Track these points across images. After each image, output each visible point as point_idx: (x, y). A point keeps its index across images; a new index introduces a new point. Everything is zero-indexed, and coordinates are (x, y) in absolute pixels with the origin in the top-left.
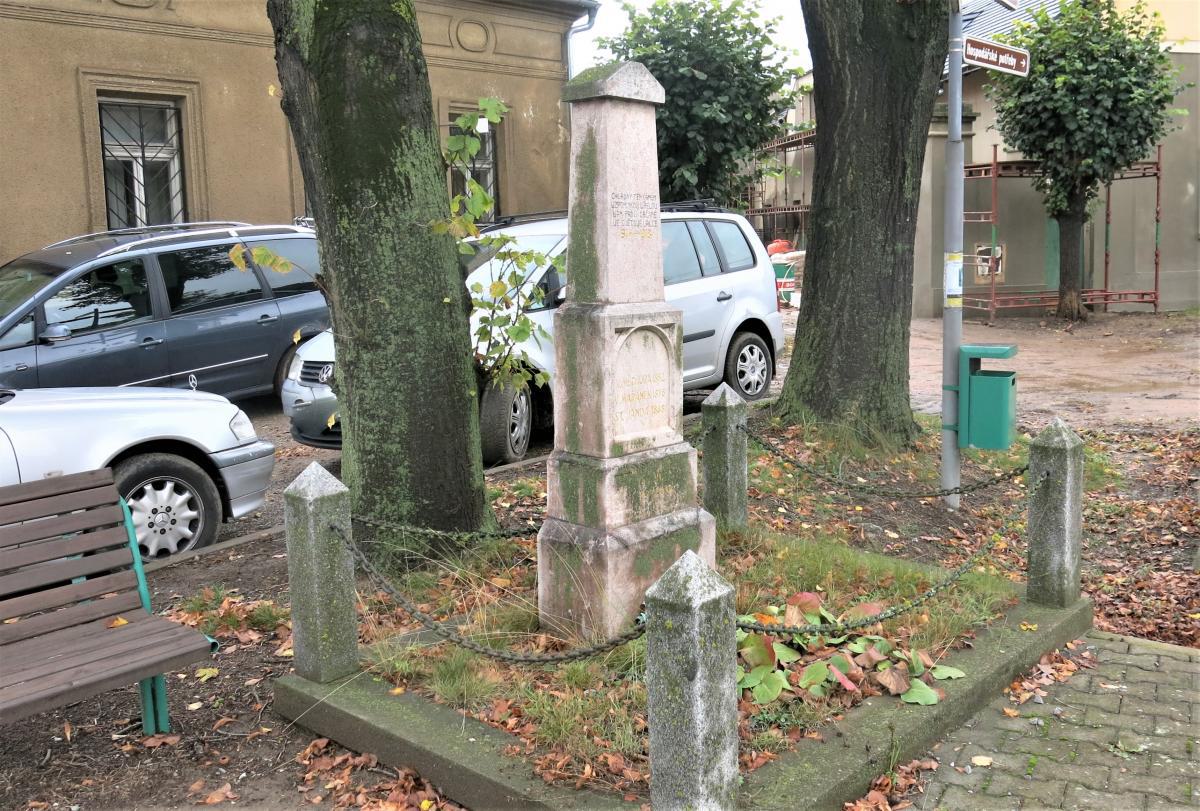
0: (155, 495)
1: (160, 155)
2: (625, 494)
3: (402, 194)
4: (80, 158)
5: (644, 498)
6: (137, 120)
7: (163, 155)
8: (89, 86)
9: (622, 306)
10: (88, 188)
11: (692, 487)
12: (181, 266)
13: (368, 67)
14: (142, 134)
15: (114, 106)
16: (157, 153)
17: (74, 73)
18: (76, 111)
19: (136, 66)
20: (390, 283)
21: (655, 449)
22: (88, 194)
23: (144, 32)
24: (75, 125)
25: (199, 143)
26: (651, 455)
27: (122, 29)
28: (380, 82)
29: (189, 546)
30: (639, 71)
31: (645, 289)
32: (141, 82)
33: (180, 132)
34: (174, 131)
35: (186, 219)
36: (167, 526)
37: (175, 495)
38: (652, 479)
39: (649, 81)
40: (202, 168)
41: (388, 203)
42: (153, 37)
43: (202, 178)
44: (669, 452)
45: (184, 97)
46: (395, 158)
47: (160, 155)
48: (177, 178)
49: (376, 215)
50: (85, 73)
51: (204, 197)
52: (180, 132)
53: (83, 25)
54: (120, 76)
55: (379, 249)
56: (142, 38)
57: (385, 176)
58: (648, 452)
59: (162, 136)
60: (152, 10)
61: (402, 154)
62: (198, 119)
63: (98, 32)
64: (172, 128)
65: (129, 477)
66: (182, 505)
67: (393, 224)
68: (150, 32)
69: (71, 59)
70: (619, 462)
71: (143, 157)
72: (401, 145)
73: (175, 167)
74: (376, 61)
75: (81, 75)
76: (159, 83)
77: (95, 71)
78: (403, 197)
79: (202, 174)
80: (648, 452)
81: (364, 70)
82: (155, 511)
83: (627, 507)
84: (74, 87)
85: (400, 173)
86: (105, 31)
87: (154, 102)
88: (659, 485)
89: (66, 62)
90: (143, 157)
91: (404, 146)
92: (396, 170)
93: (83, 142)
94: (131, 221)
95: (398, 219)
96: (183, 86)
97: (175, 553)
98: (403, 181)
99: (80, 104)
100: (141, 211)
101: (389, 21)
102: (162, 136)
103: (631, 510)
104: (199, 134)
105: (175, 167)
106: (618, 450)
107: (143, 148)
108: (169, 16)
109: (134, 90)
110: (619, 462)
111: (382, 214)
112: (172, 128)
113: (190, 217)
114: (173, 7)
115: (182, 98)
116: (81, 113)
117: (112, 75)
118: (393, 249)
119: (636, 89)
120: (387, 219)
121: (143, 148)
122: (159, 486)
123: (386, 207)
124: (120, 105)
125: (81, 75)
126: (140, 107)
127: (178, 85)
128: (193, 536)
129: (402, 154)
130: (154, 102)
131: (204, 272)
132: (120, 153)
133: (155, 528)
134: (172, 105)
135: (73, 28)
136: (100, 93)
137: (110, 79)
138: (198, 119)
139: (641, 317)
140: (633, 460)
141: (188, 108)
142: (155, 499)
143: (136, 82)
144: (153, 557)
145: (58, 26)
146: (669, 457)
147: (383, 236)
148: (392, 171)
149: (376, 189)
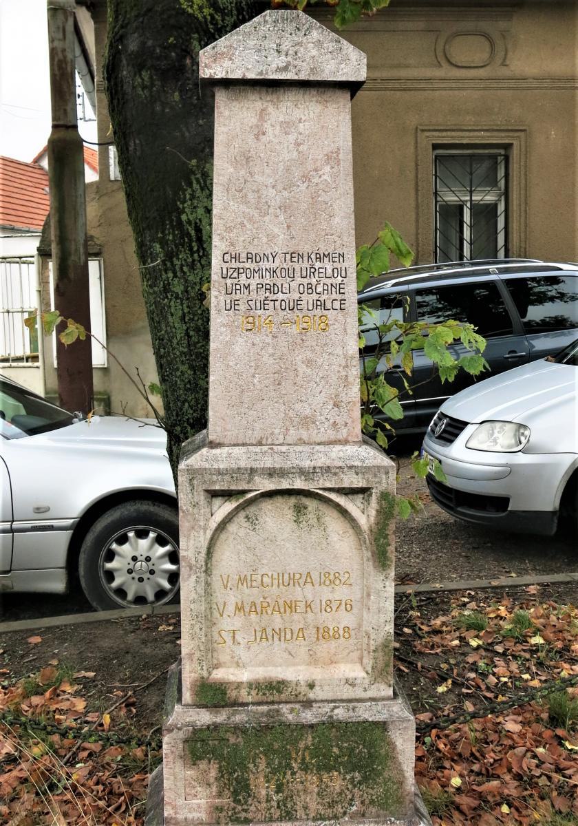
0: (137, 544)
1: (487, 198)
2: (213, 773)
3: (191, 249)
4: (413, 203)
5: (262, 788)
6: (469, 170)
7: (490, 198)
8: (426, 141)
9: (236, 450)
10: (417, 228)
11: (401, 783)
12: (523, 292)
13: (144, 88)
14: (471, 181)
15: (456, 159)
16: (487, 197)
17: (413, 132)
18: (413, 164)
19: (469, 120)
20: (183, 363)
21: (308, 704)
22: (417, 234)
23: (479, 89)
24: (411, 176)
25: (523, 185)
26: (288, 713)
27: (459, 89)
28: (164, 105)
29: (166, 600)
30: (290, 28)
31: (307, 422)
32: (471, 134)
33: (507, 176)
34: (503, 175)
35: (506, 256)
36: (146, 576)
37: (157, 546)
38: (287, 756)
39: (319, 44)
40: (523, 209)
41: (175, 261)
42: (486, 92)
43: (523, 218)
44: (340, 713)
45: (512, 144)
46: (184, 202)
47: (487, 198)
48: (503, 215)
49: (164, 276)
50: (423, 131)
51: (523, 235)
52: (507, 176)
53: (424, 89)
54: (453, 130)
55: (170, 320)
56: (476, 94)
57: (172, 227)
58: (285, 709)
59: (494, 183)
60: (488, 68)
61: (193, 197)
62: (522, 163)
63: (437, 93)
64: (501, 173)
65: (112, 522)
66: (162, 557)
67: (182, 288)
68: (485, 89)
69: (412, 120)
70: (204, 718)
71: (471, 200)
72: (190, 184)
73: (501, 207)
74: (151, 77)
75: (419, 132)
76: (488, 134)
77: (431, 128)
78: (192, 253)
79: (523, 214)
80: (285, 709)
81: (140, 91)
82: (135, 559)
83: (220, 795)
84: (413, 143)
85: (189, 222)
86: (444, 93)
87: (487, 151)
88: (305, 768)
89: (408, 122)
90: (471, 200)
91: (195, 185)
92: (184, 217)
93: (417, 190)
94: (461, 257)
95: (186, 281)
96: (511, 134)
97: (152, 603)
98: (193, 233)
99: (416, 157)
100: (466, 252)
101: (172, 21)
102: (494, 183)
103: (226, 801)
104: (523, 177)
105: (501, 207)
106: (214, 695)
107: (471, 192)
108: (504, 72)
109: (465, 141)
110: (204, 718)
111: (170, 275)
112: (501, 173)
113: (510, 253)
114: (508, 63)
115: (511, 145)
116: (417, 165)
117: (446, 130)
118: (183, 318)
119: (281, 61)
120: (176, 280)
121: (471, 192)
122: (142, 534)
123: (173, 265)
124: (453, 156)
125: (419, 132)
126: (471, 156)
127: (507, 134)
128: (171, 590)
129: (193, 197)
130: (487, 151)
131: (542, 299)
132: (451, 198)
133: (134, 574)
134: (502, 152)
135: (416, 93)
136: (435, 147)
137: (444, 134)
138: (522, 163)
139: (271, 473)
140: (240, 718)
141: (515, 152)
142: (135, 548)
143: (467, 134)
144: (130, 602)
145: (403, 93)
146: (332, 724)
147: (172, 303)
148: (180, 222)
149: (163, 243)
